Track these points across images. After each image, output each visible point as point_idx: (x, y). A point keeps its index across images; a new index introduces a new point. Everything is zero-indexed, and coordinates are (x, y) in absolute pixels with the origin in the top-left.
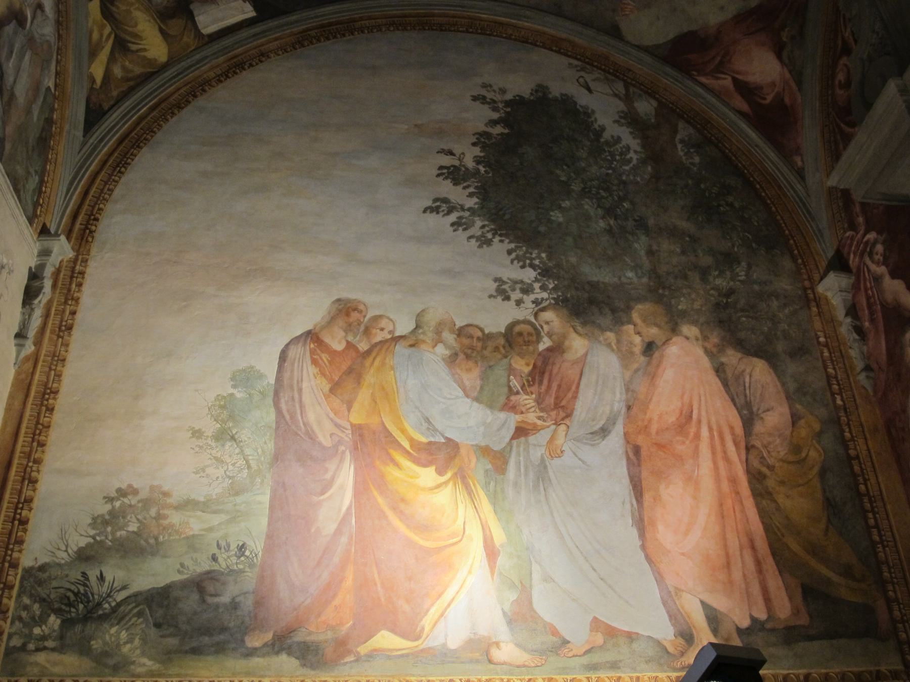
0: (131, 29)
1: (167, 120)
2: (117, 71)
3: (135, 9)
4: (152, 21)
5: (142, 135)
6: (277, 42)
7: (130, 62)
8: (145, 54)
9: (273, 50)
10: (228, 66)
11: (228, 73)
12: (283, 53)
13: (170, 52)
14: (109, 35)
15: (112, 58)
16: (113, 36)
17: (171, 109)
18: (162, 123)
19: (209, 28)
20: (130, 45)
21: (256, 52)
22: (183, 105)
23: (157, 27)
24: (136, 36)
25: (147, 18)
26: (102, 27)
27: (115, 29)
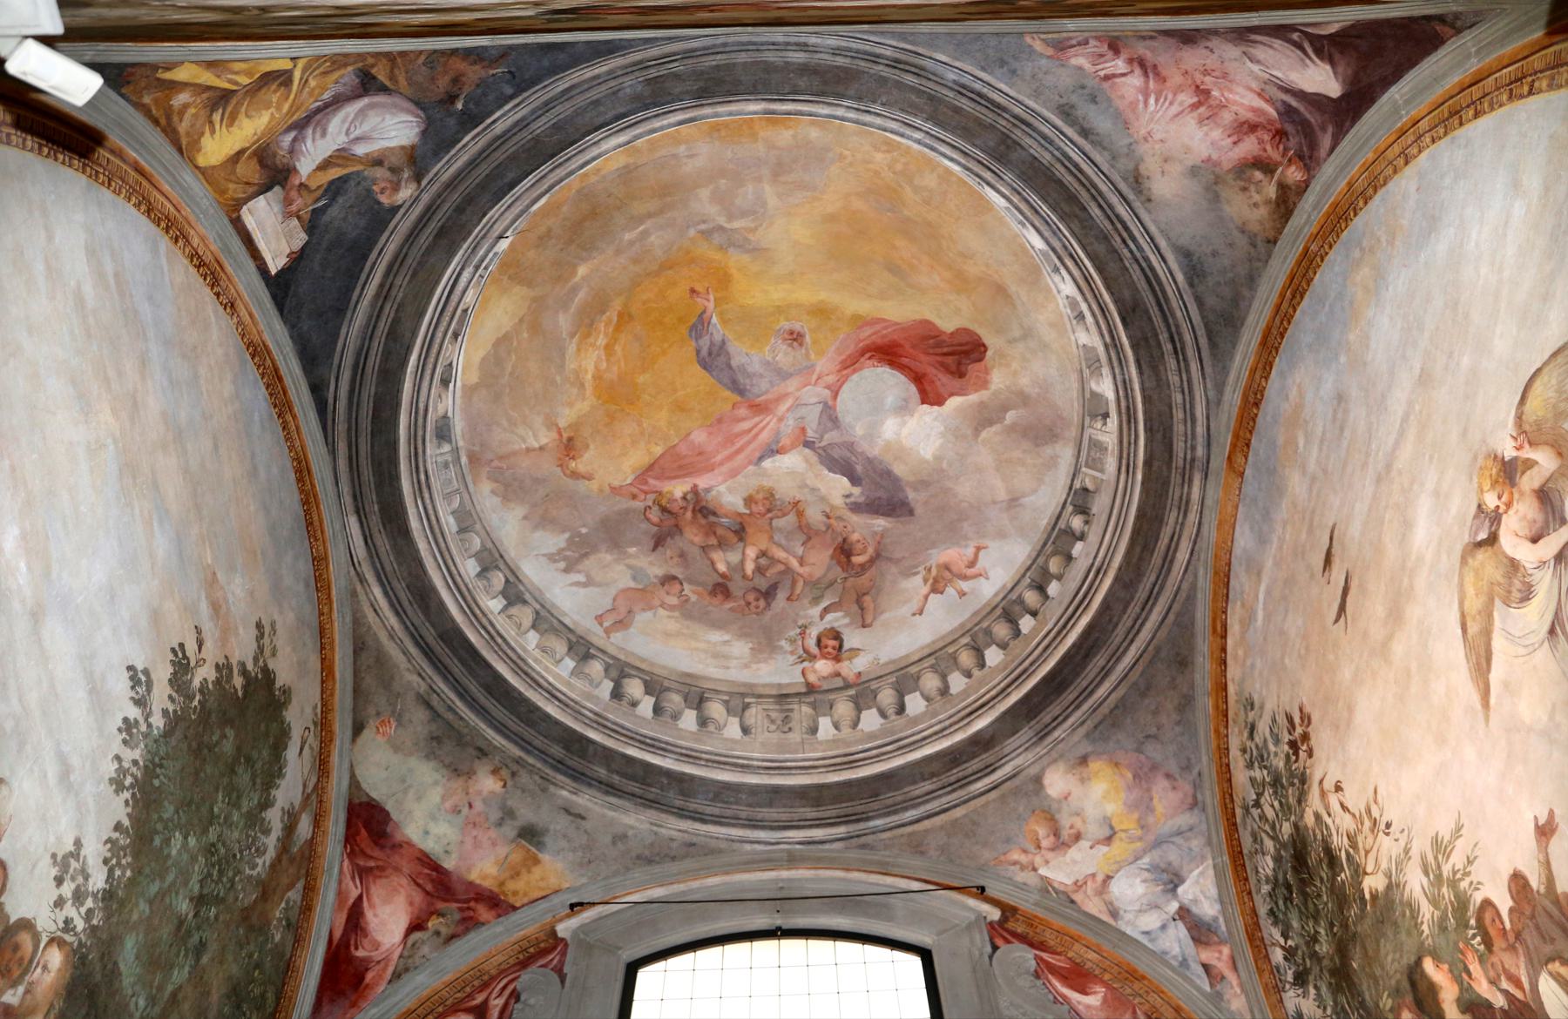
0: (243, 110)
5: (101, 165)
8: (207, 134)
14: (236, 83)
16: (235, 88)
20: (220, 111)
24: (232, 119)
25: (259, 132)
26: (248, 73)
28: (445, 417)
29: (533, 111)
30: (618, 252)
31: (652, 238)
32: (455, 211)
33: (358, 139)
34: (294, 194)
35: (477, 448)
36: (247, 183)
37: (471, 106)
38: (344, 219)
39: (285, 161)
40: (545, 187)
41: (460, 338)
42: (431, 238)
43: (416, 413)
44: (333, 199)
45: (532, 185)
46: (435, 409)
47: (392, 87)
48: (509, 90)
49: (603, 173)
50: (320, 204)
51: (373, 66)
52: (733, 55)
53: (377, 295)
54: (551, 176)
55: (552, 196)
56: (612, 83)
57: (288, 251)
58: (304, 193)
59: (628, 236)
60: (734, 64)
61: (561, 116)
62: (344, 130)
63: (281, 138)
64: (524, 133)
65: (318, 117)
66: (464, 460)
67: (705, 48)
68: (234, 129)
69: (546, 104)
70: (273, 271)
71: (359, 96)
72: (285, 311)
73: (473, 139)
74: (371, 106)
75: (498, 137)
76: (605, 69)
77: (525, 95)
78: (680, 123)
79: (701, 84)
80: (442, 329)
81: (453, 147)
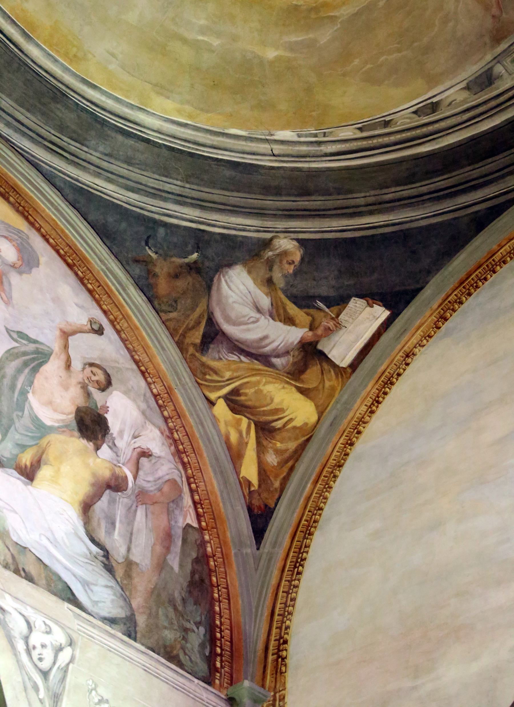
1: (331, 488)
2: (271, 459)
3: (264, 385)
4: (286, 386)
6: (419, 331)
7: (281, 443)
9: (417, 343)
10: (377, 389)
11: (378, 397)
12: (428, 341)
13: (317, 406)
15: (261, 448)
16: (253, 426)
17: (332, 472)
18: (326, 493)
19: (348, 357)
20: (273, 424)
21: (400, 356)
22: (343, 461)
23: (294, 389)
25: (281, 386)
27: (251, 417)
28: (468, 88)
29: (165, 200)
30: (235, 38)
31: (203, 22)
32: (281, 195)
33: (259, 310)
34: (319, 332)
35: (487, 39)
36: (322, 374)
37: (190, 248)
38: (326, 278)
39: (297, 353)
40: (220, 139)
41: (388, 119)
42: (313, 198)
43: (474, 118)
44: (313, 298)
45: (225, 150)
46: (465, 101)
47: (206, 317)
48: (161, 231)
49: (179, 106)
50: (321, 305)
51: (194, 345)
52: (11, 110)
53: (380, 212)
54: (208, 142)
55: (225, 127)
56: (105, 165)
57: (368, 309)
58: (317, 323)
59: (216, 42)
60: (16, 101)
61: (157, 177)
62: (256, 325)
63: (280, 367)
64: (187, 192)
65: (253, 351)
66: (504, 46)
67: (24, 134)
68: (284, 406)
69: (154, 196)
70: (387, 313)
71: (224, 334)
72: (418, 286)
73: (214, 226)
74: (228, 319)
75: (203, 208)
76: (98, 181)
77: (157, 217)
78: (94, 87)
79: (53, 105)
80: (386, 140)
81: (229, 235)
